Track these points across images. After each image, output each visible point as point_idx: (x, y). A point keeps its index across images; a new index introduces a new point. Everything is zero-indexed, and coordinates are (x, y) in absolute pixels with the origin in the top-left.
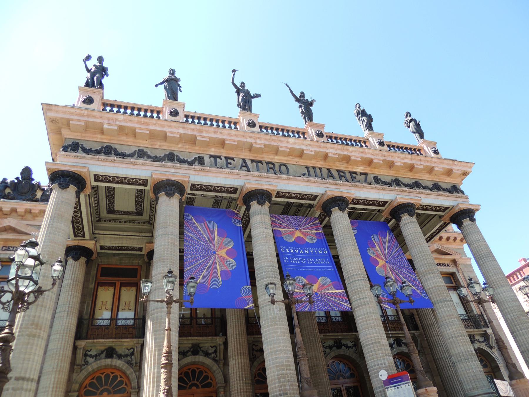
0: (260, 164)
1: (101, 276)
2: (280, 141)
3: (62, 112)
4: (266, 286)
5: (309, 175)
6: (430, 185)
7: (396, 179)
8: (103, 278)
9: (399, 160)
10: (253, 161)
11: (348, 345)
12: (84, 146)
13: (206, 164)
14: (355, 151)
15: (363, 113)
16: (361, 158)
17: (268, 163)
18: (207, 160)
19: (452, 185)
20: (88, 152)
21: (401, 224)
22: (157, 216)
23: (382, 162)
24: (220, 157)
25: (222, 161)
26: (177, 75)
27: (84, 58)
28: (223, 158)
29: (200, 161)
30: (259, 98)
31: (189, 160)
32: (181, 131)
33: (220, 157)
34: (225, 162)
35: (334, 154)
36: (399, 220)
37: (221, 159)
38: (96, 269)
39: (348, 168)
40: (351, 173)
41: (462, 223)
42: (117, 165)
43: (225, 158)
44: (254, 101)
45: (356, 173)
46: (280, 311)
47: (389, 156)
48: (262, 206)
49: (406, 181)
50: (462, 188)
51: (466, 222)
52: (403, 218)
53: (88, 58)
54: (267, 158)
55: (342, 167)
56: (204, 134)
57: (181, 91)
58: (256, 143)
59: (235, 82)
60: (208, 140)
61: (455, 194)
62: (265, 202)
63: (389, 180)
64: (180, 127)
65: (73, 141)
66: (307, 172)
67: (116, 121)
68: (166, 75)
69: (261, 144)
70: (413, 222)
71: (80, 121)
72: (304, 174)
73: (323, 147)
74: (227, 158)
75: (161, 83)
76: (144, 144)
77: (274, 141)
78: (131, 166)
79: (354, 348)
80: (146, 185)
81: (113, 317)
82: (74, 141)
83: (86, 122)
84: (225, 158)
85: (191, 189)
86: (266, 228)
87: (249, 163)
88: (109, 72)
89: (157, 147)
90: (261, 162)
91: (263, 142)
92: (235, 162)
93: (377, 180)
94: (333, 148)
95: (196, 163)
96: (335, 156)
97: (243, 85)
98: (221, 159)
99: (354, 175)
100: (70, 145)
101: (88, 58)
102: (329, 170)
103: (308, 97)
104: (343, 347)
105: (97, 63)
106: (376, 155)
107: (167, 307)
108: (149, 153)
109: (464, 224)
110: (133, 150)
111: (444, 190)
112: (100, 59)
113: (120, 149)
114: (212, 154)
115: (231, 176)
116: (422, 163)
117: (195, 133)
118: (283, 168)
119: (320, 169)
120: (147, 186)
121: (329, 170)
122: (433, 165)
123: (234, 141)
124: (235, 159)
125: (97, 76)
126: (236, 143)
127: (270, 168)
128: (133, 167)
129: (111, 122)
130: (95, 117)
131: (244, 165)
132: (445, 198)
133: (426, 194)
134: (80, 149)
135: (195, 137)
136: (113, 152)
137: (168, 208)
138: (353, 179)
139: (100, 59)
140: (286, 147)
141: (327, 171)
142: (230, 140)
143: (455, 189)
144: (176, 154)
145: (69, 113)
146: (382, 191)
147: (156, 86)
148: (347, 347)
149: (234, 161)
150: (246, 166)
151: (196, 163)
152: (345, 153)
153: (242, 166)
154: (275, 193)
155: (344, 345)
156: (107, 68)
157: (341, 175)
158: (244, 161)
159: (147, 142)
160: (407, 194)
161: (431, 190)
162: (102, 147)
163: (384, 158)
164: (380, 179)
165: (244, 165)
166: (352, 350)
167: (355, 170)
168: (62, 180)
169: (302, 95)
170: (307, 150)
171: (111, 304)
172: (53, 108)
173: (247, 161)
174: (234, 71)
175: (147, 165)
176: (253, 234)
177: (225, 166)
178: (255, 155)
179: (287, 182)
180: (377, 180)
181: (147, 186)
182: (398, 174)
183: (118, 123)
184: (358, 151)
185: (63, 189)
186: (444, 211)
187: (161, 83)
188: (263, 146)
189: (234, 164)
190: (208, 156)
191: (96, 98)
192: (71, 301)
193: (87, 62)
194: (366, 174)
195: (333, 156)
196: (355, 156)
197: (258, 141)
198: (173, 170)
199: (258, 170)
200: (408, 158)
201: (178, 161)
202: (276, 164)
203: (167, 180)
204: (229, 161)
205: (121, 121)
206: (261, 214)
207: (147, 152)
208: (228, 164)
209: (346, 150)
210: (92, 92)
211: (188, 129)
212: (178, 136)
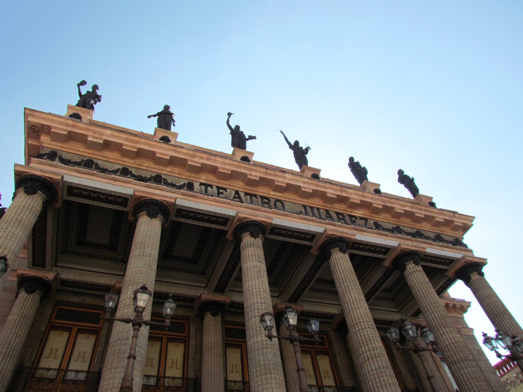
0: (254, 198)
1: (56, 318)
2: (276, 175)
3: (45, 119)
4: (263, 316)
5: (306, 214)
6: (432, 236)
7: (396, 227)
8: (60, 321)
9: (399, 207)
10: (246, 194)
12: (63, 157)
13: (195, 190)
14: (355, 194)
16: (361, 201)
17: (262, 198)
18: (197, 186)
19: (455, 238)
20: (65, 162)
21: (406, 273)
22: (135, 235)
23: (381, 207)
24: (211, 186)
25: (213, 190)
26: (171, 110)
28: (214, 187)
29: (190, 186)
30: (254, 140)
31: (177, 185)
32: (172, 154)
33: (211, 186)
34: (216, 191)
35: (333, 194)
36: (403, 268)
37: (212, 188)
38: (51, 308)
39: (347, 211)
40: (350, 216)
41: (470, 278)
42: (95, 178)
43: (217, 187)
44: (248, 143)
45: (355, 217)
46: (275, 357)
47: (389, 202)
48: (255, 238)
49: (408, 230)
50: (465, 241)
51: (474, 276)
52: (408, 267)
53: (83, 83)
54: (262, 191)
55: (340, 208)
56: (196, 160)
57: (174, 125)
58: (251, 175)
59: (230, 123)
60: (200, 166)
61: (458, 247)
62: (258, 234)
63: (390, 226)
64: (170, 150)
65: (50, 150)
66: (304, 211)
67: (102, 135)
68: (161, 109)
69: (256, 176)
70: (419, 270)
71: (63, 130)
72: (301, 213)
73: (321, 187)
74: (218, 188)
75: (154, 116)
76: (129, 163)
77: (270, 174)
78: (112, 182)
80: (126, 206)
81: (62, 368)
82: (53, 150)
83: (70, 132)
84: (217, 187)
85: (176, 216)
86: (259, 261)
87: (242, 195)
88: (103, 99)
89: (144, 168)
90: (255, 196)
91: (258, 174)
92: (227, 193)
93: (377, 226)
94: (332, 188)
95: (185, 188)
96: (333, 196)
97: (237, 127)
98: (212, 188)
99: (353, 219)
100: (47, 154)
101: (83, 83)
102: (327, 211)
103: (303, 145)
106: (376, 200)
107: (134, 330)
108: (134, 172)
109: (473, 278)
110: (117, 167)
111: (447, 242)
112: (95, 87)
113: (101, 164)
114: (203, 181)
115: (222, 205)
116: (423, 212)
117: (187, 157)
118: (278, 204)
119: (318, 209)
120: (126, 207)
121: (327, 211)
122: (433, 215)
123: (229, 170)
124: (227, 190)
125: (89, 100)
126: (230, 173)
127: (265, 203)
128: (114, 183)
129: (96, 135)
130: (81, 129)
131: (237, 196)
132: (450, 250)
133: (430, 244)
134: (57, 159)
135: (186, 160)
136: (94, 167)
137: (148, 232)
138: (353, 222)
139: (95, 87)
140: (282, 182)
141: (325, 212)
142: (223, 169)
143: (458, 243)
144: (163, 177)
145: (53, 121)
146: (384, 237)
147: (149, 117)
149: (226, 191)
150: (239, 198)
151: (185, 188)
152: (344, 194)
153: (235, 197)
154: (270, 228)
156: (100, 96)
157: (340, 216)
158: (237, 192)
159: (133, 161)
160: (410, 242)
161: (434, 240)
162: (83, 161)
163: (384, 204)
164: (381, 226)
165: (237, 196)
168: (29, 185)
169: (297, 143)
170: (305, 188)
171: (63, 353)
172: (36, 114)
173: (240, 193)
174: (230, 114)
175: (130, 183)
176: (243, 268)
177: (216, 195)
178: (250, 188)
179: (283, 217)
180: (377, 226)
181: (126, 207)
182: (400, 222)
183: (104, 137)
184: (357, 194)
185: (28, 194)
186: (448, 264)
187: (154, 116)
188: (258, 179)
189: (226, 194)
190: (199, 183)
191: (85, 117)
192: (13, 341)
193: (81, 87)
194: (366, 219)
195: (331, 196)
196: (354, 199)
197: (254, 173)
199: (252, 202)
200: (408, 206)
202: (271, 199)
203: (150, 199)
204: (221, 191)
205: (107, 136)
206: (254, 246)
207: (132, 172)
208: (219, 193)
209: (345, 191)
210: (81, 111)
211: (179, 152)
212: (168, 158)
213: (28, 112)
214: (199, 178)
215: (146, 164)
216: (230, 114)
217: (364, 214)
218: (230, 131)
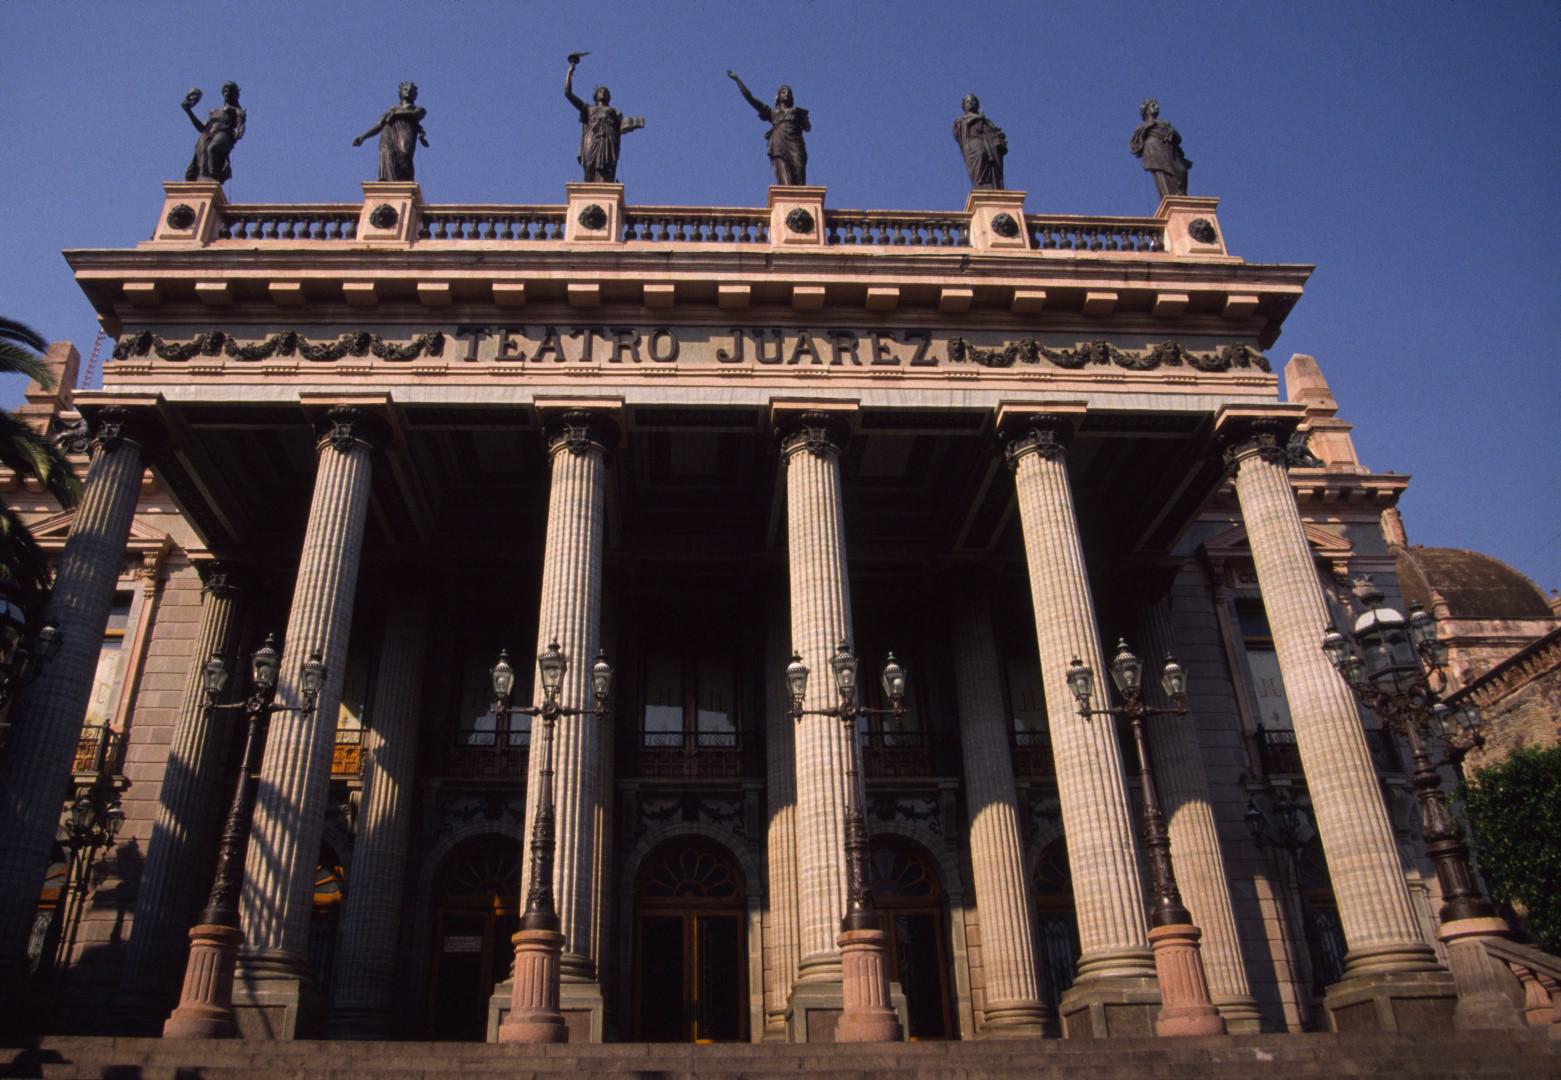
11: (917, 810)
15: (980, 126)
27: (183, 99)
53: (193, 99)
57: (425, 144)
59: (574, 92)
79: (931, 819)
89: (328, 321)
101: (193, 99)
104: (900, 816)
105: (222, 107)
112: (232, 93)
114: (466, 321)
134: (153, 349)
139: (232, 93)
147: (358, 142)
148: (910, 814)
155: (902, 810)
166: (922, 824)
167: (887, 325)
174: (574, 59)
193: (193, 110)
198: (357, 380)
201: (375, 353)
213: (75, 260)
214: (458, 316)
215: (330, 310)
216: (574, 59)
217: (920, 320)
218: (577, 113)
